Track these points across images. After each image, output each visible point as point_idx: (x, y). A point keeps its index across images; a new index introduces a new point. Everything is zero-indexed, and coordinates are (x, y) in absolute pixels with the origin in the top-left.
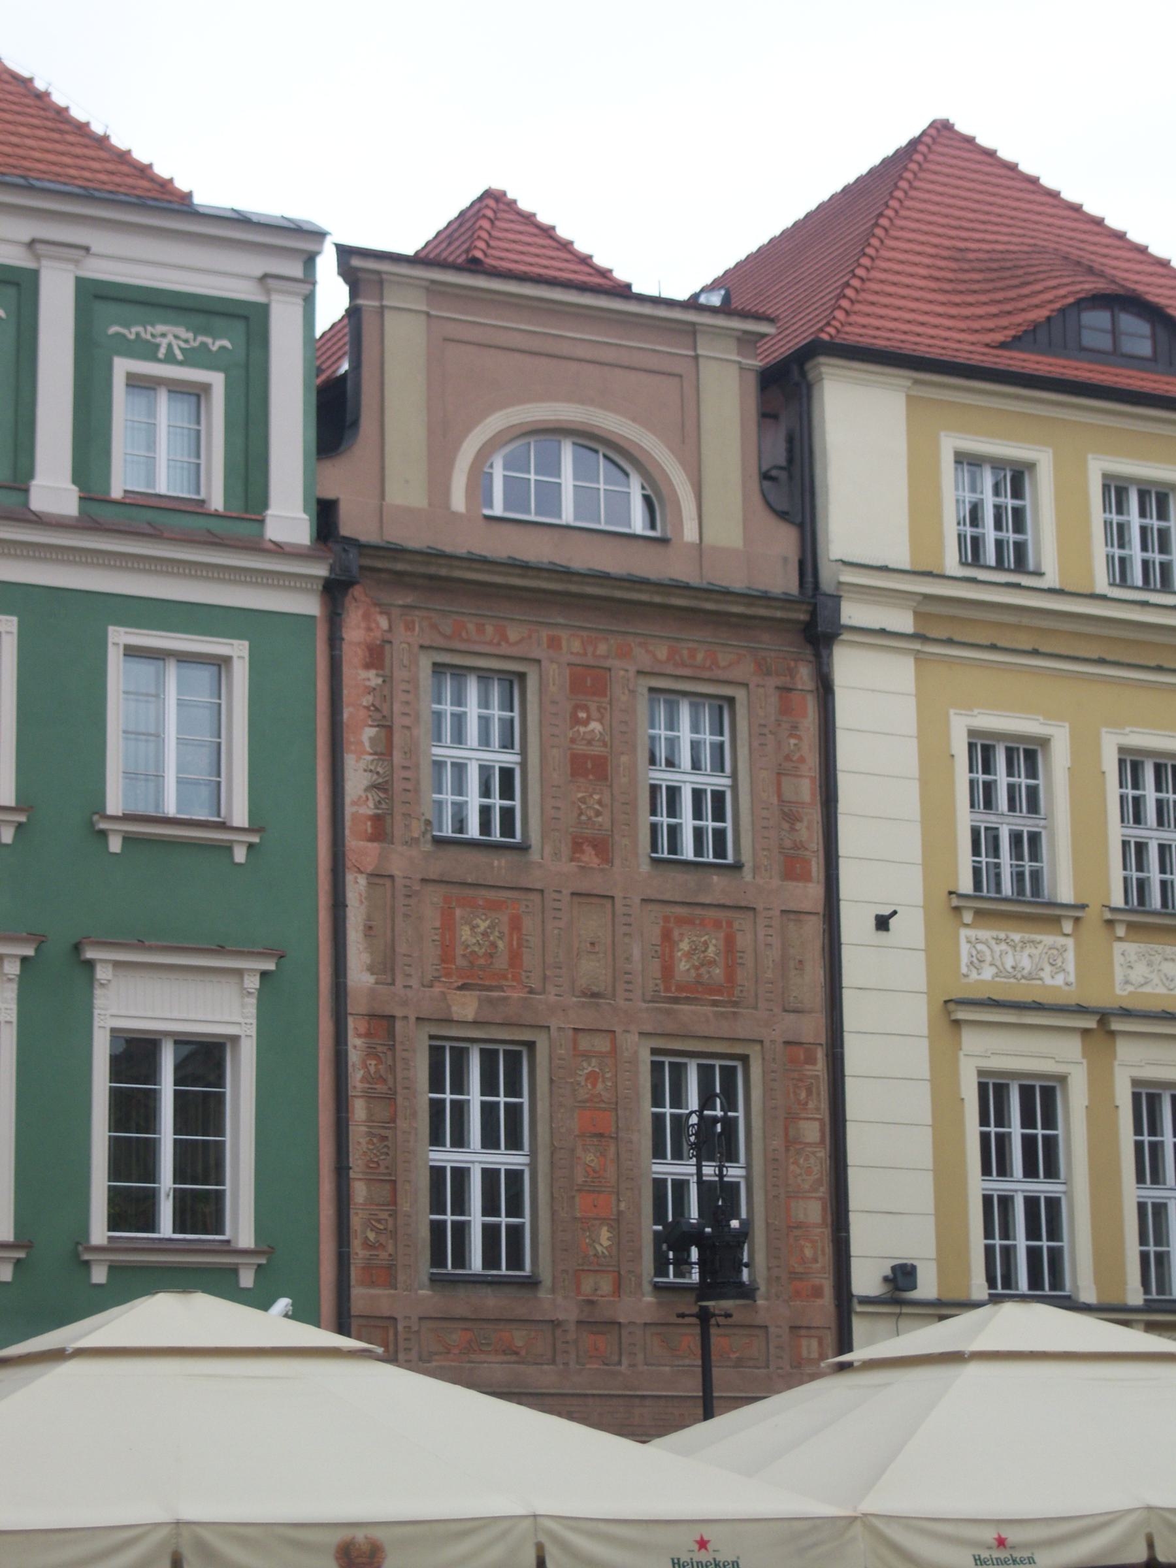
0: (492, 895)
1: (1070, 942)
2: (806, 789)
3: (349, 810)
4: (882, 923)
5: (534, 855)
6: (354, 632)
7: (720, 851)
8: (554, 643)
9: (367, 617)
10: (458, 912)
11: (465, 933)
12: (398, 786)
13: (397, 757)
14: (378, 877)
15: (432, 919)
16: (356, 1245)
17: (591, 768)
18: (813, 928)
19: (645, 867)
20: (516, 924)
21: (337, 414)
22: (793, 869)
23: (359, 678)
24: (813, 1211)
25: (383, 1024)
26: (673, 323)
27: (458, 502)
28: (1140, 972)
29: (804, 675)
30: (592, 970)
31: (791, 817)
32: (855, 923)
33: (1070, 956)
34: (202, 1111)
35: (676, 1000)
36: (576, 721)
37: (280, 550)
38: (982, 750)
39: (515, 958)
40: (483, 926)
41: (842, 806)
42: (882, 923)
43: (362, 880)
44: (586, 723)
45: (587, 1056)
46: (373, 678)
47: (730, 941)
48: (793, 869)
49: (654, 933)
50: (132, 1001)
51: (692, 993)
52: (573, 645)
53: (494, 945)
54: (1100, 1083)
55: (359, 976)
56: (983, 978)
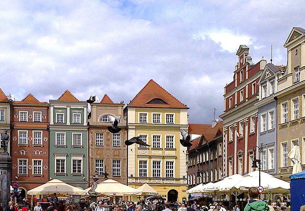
3: (90, 144)
5: (104, 146)
7: (119, 145)
11: (98, 152)
16: (90, 173)
21: (89, 116)
24: (125, 171)
26: (117, 105)
27: (99, 121)
29: (126, 132)
30: (108, 154)
33: (148, 152)
34: (79, 165)
45: (107, 160)
46: (92, 135)
47: (119, 152)
49: (113, 151)
54: (150, 161)
56: (140, 154)
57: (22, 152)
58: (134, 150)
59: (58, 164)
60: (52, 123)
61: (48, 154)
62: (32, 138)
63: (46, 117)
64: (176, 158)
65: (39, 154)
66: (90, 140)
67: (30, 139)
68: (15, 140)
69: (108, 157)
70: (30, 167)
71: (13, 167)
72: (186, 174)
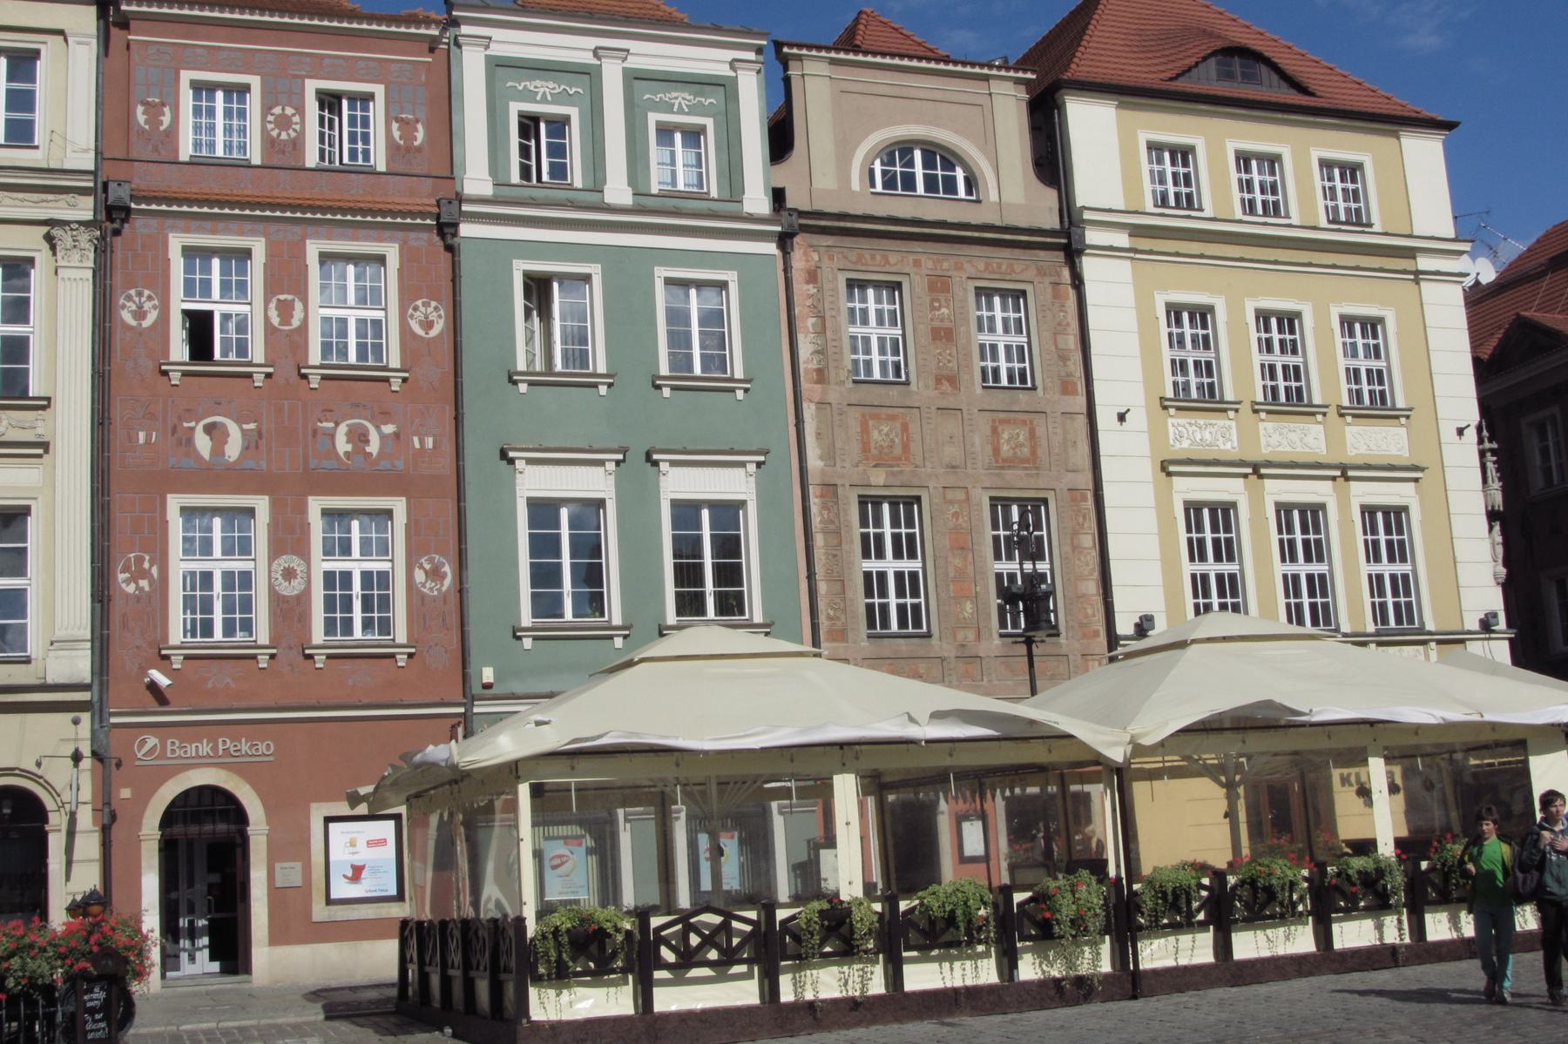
0: (890, 411)
1: (1233, 424)
2: (1072, 341)
4: (1121, 418)
5: (913, 387)
6: (798, 260)
8: (917, 263)
9: (805, 254)
10: (871, 423)
11: (875, 435)
12: (831, 351)
13: (829, 334)
14: (822, 404)
15: (855, 427)
17: (943, 335)
18: (1082, 421)
19: (979, 390)
20: (905, 428)
22: (1067, 388)
23: (802, 289)
25: (830, 489)
27: (856, 185)
28: (1276, 438)
30: (951, 452)
31: (1064, 358)
32: (1105, 418)
33: (1234, 431)
35: (1002, 468)
36: (934, 308)
37: (751, 218)
38: (1175, 312)
39: (906, 447)
40: (886, 430)
41: (1093, 351)
42: (1121, 418)
43: (813, 407)
44: (939, 309)
45: (951, 502)
46: (812, 289)
47: (1032, 433)
48: (1067, 388)
49: (987, 430)
50: (681, 482)
51: (1012, 463)
52: (928, 264)
53: (893, 441)
55: (814, 462)
57: (209, 429)
58: (1137, 419)
59: (544, 546)
60: (476, 179)
61: (448, 447)
62: (298, 305)
63: (420, 135)
64: (1410, 471)
65: (374, 447)
66: (801, 338)
67: (285, 310)
68: (146, 323)
69: (951, 481)
70: (289, 574)
71: (122, 577)
72: (1494, 601)
